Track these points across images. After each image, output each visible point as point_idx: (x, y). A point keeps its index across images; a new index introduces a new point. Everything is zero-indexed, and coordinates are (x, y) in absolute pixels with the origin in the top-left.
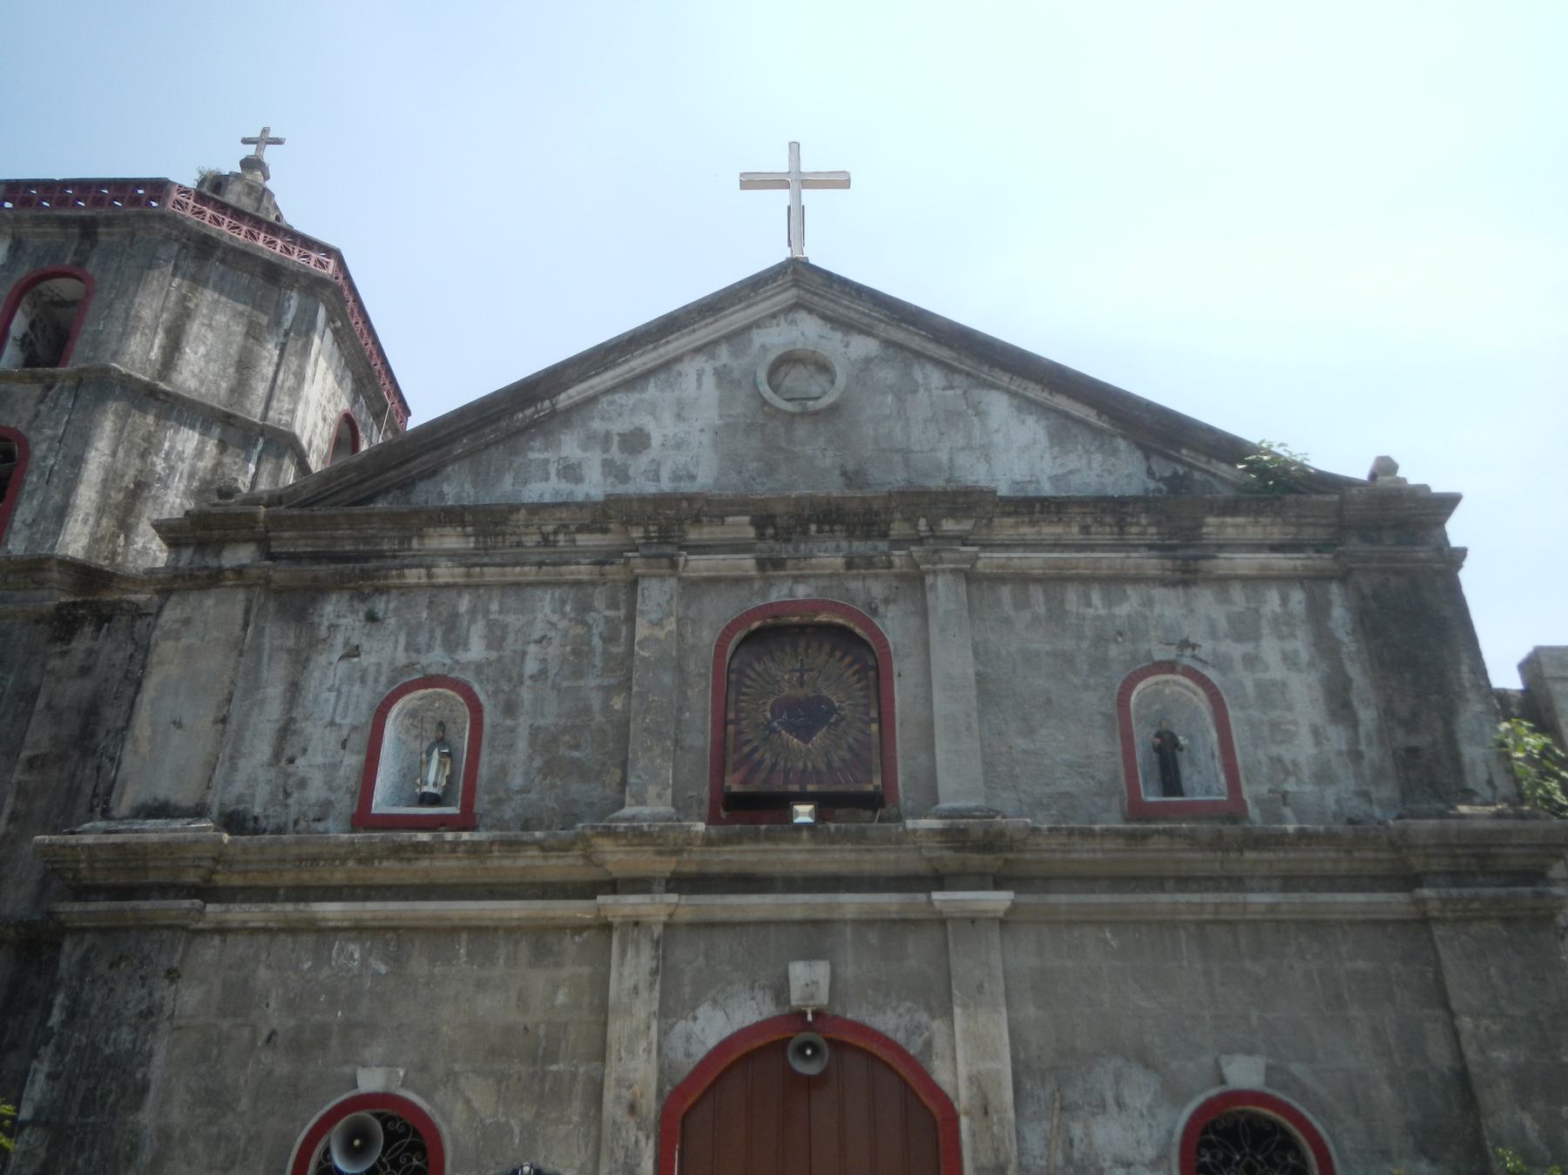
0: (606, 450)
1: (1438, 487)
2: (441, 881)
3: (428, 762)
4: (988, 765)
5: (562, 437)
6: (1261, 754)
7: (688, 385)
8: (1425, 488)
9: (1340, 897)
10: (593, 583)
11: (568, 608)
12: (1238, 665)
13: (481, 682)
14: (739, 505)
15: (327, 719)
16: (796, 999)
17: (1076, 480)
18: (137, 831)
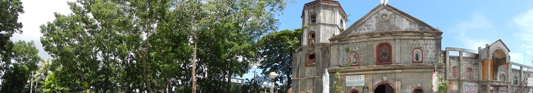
4: (401, 58)
12: (425, 48)
16: (384, 80)
17: (411, 28)
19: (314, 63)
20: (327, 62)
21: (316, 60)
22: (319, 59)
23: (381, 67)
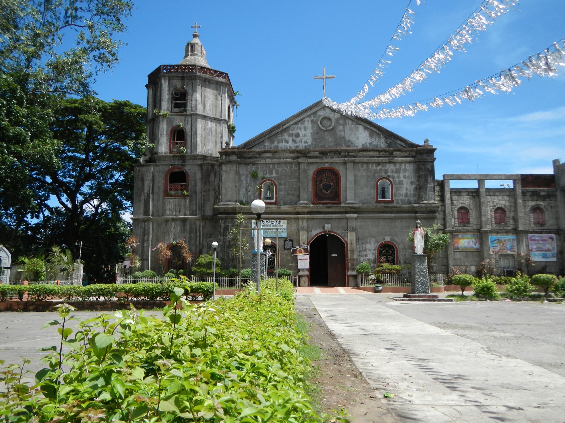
0: (292, 137)
1: (434, 147)
4: (355, 194)
6: (397, 192)
7: (306, 123)
8: (432, 146)
9: (405, 215)
10: (292, 163)
12: (396, 178)
14: (317, 151)
16: (326, 229)
17: (373, 143)
18: (228, 205)
19: (185, 192)
20: (212, 193)
21: (190, 186)
22: (195, 185)
23: (320, 207)
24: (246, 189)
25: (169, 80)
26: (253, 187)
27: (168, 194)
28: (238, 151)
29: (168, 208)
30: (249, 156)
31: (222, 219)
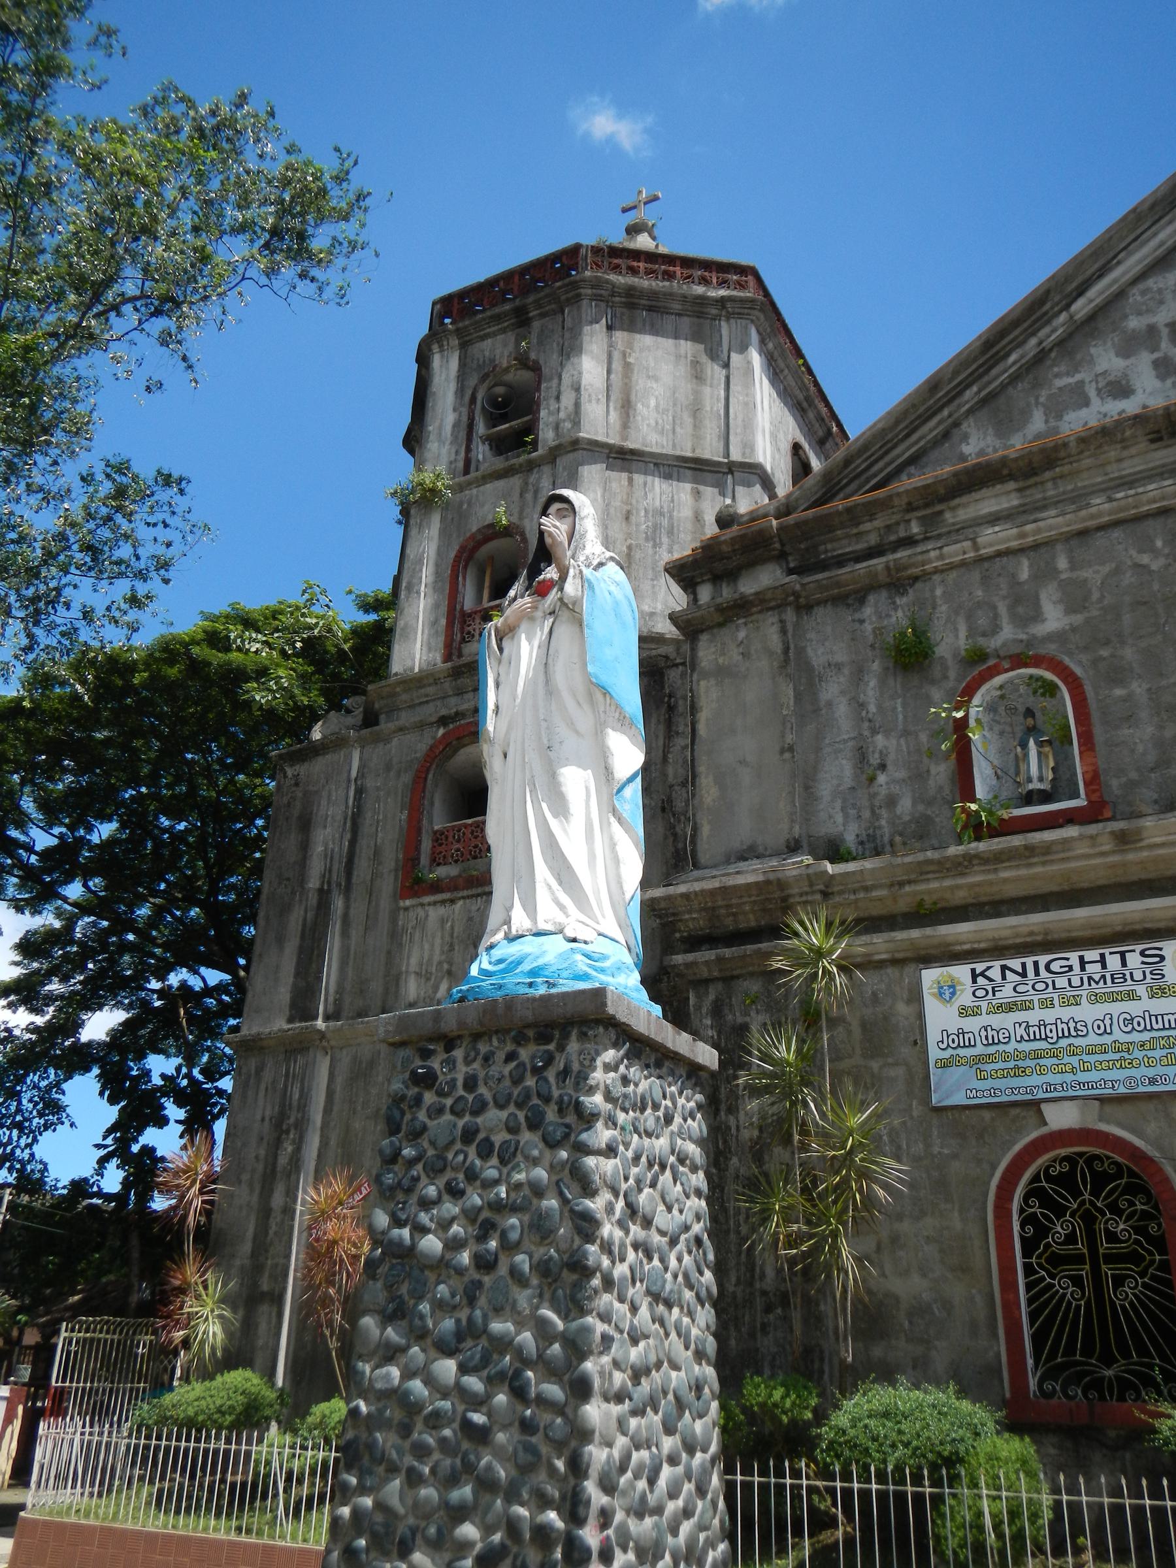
2: (1086, 885)
3: (1026, 756)
5: (1093, 351)
11: (1159, 543)
13: (1070, 654)
15: (901, 727)
24: (861, 755)
25: (464, 346)
26: (906, 733)
27: (418, 881)
28: (781, 528)
29: (414, 961)
30: (860, 546)
31: (703, 983)
